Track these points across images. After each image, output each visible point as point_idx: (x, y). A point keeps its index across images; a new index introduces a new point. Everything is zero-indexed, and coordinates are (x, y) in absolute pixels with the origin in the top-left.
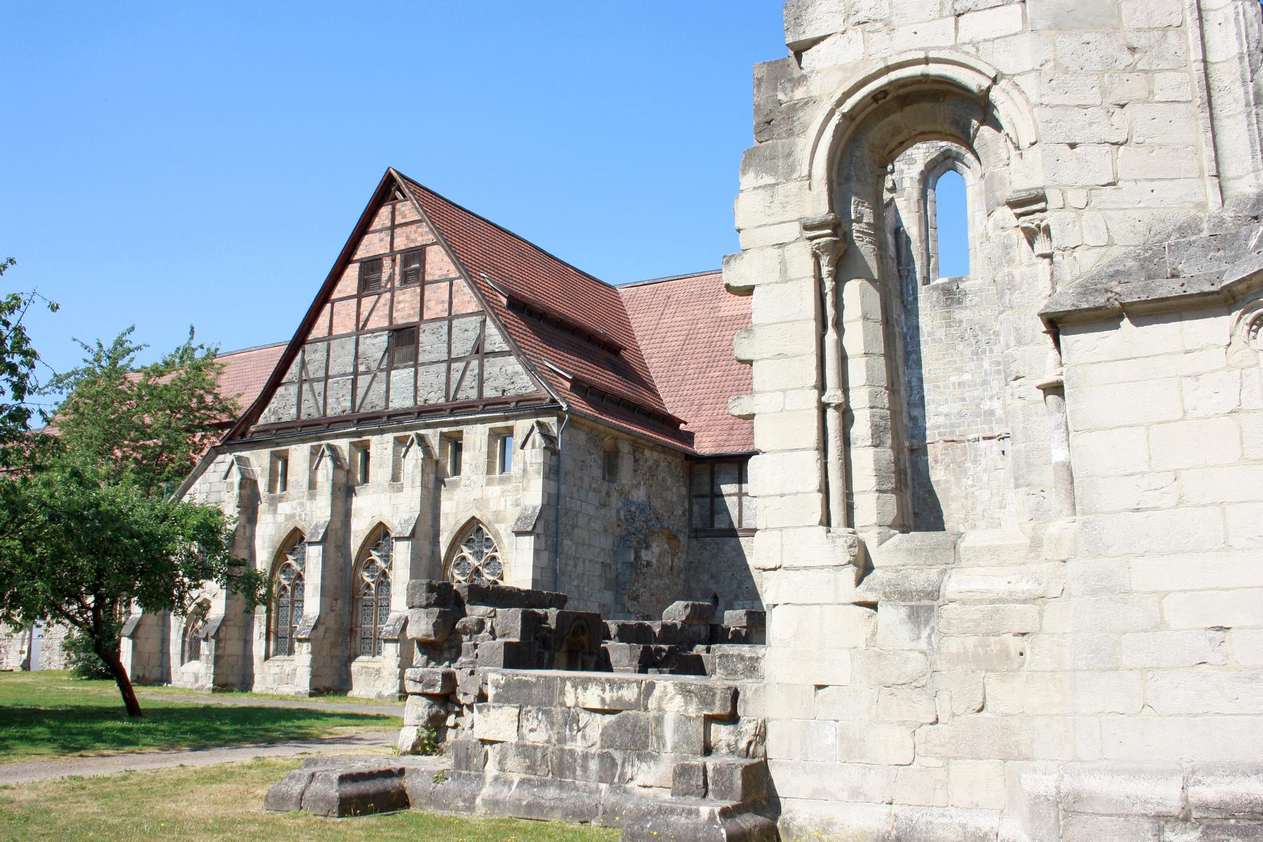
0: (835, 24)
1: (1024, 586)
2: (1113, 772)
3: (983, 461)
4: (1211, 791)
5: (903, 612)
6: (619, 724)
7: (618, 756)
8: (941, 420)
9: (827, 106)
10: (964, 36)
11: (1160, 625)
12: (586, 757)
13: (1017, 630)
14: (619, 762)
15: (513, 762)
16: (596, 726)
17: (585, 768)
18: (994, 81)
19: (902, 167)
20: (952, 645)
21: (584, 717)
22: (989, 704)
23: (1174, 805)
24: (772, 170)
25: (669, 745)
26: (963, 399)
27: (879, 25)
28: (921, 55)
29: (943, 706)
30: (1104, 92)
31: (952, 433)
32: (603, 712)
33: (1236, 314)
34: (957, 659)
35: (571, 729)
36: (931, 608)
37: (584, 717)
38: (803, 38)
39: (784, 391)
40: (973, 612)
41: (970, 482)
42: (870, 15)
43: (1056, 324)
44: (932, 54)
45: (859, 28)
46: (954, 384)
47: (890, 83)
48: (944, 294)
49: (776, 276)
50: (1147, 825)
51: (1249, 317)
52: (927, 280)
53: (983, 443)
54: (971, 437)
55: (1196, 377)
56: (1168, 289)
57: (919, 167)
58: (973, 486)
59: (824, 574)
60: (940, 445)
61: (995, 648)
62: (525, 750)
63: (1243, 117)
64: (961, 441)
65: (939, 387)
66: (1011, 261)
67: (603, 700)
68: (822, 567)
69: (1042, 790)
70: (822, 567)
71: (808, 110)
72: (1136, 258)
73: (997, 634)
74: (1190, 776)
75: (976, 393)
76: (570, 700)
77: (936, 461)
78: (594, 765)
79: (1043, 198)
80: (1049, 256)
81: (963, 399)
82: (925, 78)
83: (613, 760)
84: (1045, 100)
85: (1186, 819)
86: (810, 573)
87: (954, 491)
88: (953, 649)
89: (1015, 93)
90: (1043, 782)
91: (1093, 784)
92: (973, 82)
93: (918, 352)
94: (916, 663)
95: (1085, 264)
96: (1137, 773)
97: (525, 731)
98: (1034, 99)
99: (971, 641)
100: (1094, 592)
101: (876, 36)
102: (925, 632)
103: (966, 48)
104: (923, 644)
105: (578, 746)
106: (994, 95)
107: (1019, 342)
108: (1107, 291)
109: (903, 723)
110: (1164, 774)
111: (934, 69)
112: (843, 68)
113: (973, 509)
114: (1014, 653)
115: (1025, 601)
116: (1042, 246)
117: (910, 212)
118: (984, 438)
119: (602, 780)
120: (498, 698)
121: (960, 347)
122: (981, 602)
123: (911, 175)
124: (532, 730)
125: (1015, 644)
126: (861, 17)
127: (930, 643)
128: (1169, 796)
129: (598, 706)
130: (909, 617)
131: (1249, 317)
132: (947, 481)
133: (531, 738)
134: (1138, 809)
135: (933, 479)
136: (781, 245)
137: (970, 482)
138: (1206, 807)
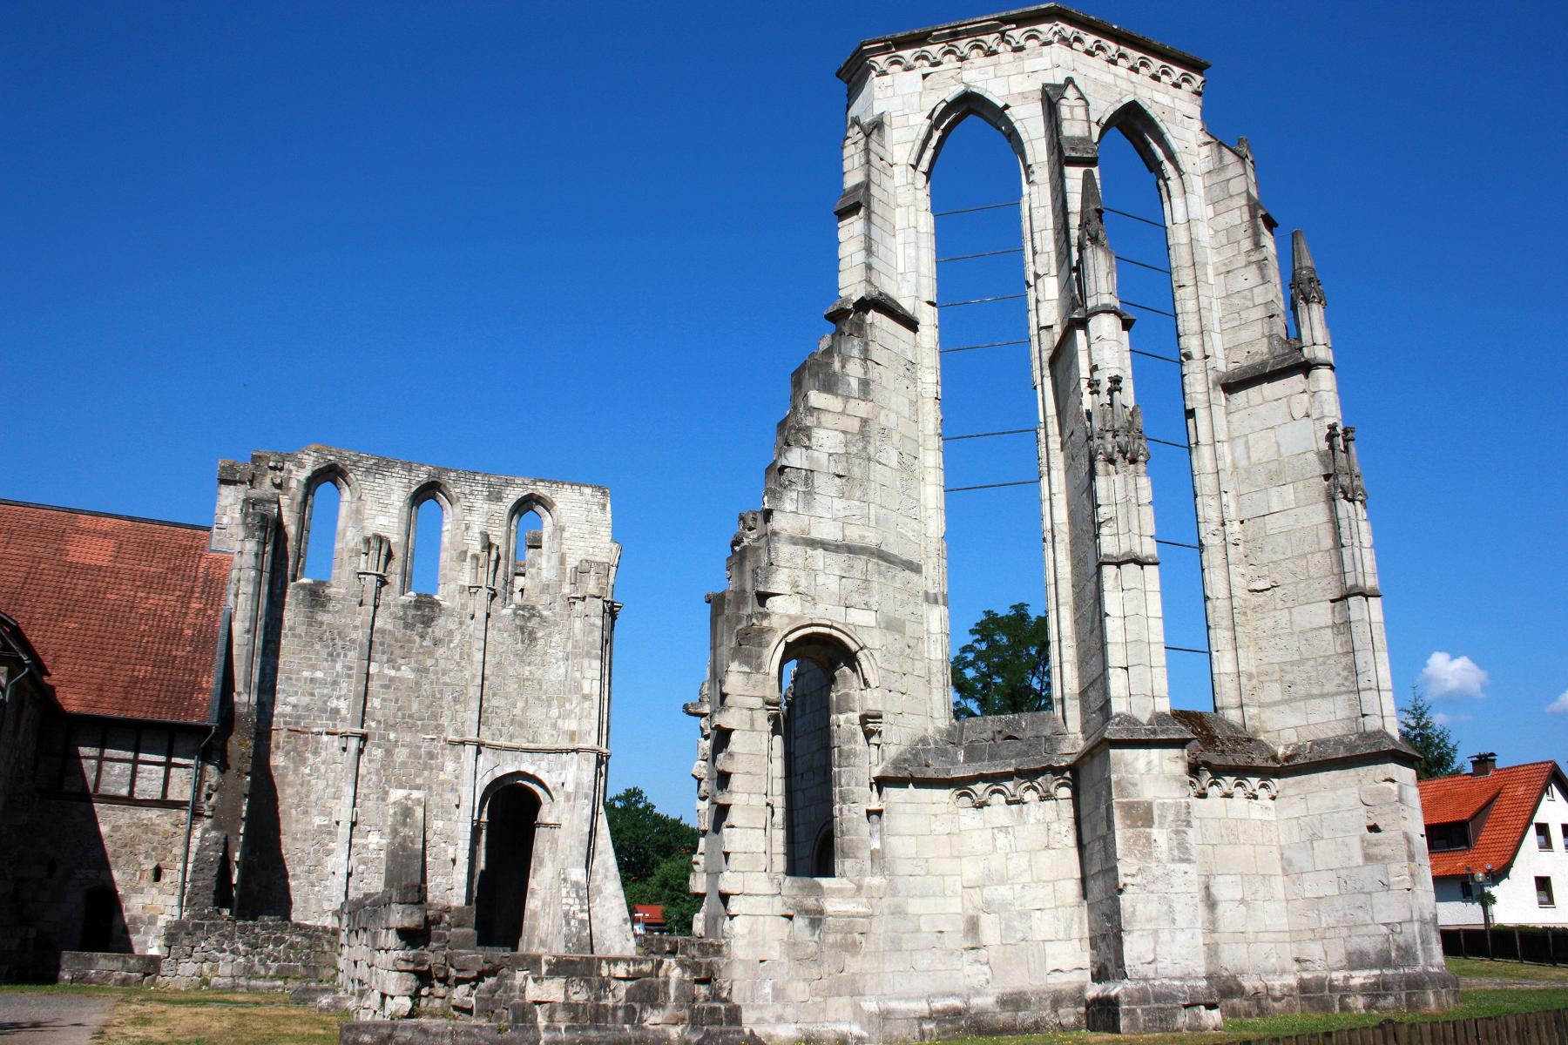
0: (785, 589)
1: (862, 910)
2: (899, 999)
3: (323, 754)
4: (939, 1004)
5: (807, 921)
6: (640, 986)
7: (637, 1006)
8: (288, 709)
9: (780, 635)
10: (850, 620)
11: (918, 930)
12: (615, 1008)
13: (860, 931)
14: (638, 1010)
15: (559, 1015)
16: (622, 989)
17: (614, 1016)
18: (861, 649)
19: (292, 468)
20: (830, 939)
21: (614, 984)
22: (846, 970)
23: (926, 1012)
24: (748, 664)
25: (672, 998)
26: (312, 695)
27: (809, 598)
28: (830, 623)
29: (825, 969)
30: (901, 667)
31: (297, 723)
32: (625, 979)
33: (952, 790)
34: (832, 946)
35: (605, 991)
36: (821, 919)
37: (614, 984)
38: (769, 591)
39: (749, 794)
40: (841, 922)
41: (307, 771)
42: (805, 590)
43: (881, 783)
44: (835, 625)
45: (799, 596)
46: (306, 679)
47: (813, 634)
48: (311, 595)
49: (747, 727)
50: (916, 1022)
51: (958, 792)
52: (294, 579)
53: (325, 738)
54: (315, 730)
55: (936, 816)
56: (930, 773)
57: (304, 474)
58: (310, 775)
59: (766, 899)
60: (284, 733)
61: (850, 941)
62: (569, 1007)
63: (941, 690)
64: (304, 733)
65: (291, 679)
66: (856, 742)
67: (628, 972)
68: (765, 895)
69: (873, 1010)
70: (765, 895)
71: (771, 633)
72: (910, 752)
73: (851, 933)
74: (929, 998)
75: (326, 691)
76: (605, 972)
77: (278, 747)
78: (620, 1013)
79: (881, 717)
80: (878, 746)
81: (312, 695)
82: (830, 636)
83: (634, 1009)
84: (883, 665)
85: (930, 1018)
86: (759, 898)
87: (291, 777)
88: (831, 941)
89: (870, 658)
90: (871, 1006)
91: (893, 1005)
92: (854, 647)
93: (278, 643)
94: (812, 948)
95: (892, 752)
96: (907, 999)
97: (570, 993)
98: (879, 664)
99: (839, 937)
100: (893, 914)
101: (808, 605)
102: (817, 933)
103: (851, 627)
104: (816, 938)
105: (610, 1002)
106: (860, 655)
107: (857, 785)
108: (906, 769)
109: (805, 980)
110: (919, 999)
111: (835, 633)
112: (789, 616)
113: (307, 796)
114: (858, 942)
115: (864, 917)
116: (875, 740)
117: (291, 511)
118: (327, 733)
119: (626, 1023)
120: (549, 972)
121: (317, 647)
122: (844, 917)
123: (299, 478)
124: (575, 993)
125: (858, 937)
126: (800, 589)
127: (819, 937)
128: (922, 1007)
129: (625, 976)
130: (810, 923)
131: (958, 792)
132: (285, 767)
133: (575, 998)
134: (913, 1015)
135: (272, 763)
136: (751, 709)
137: (307, 771)
138: (938, 1012)
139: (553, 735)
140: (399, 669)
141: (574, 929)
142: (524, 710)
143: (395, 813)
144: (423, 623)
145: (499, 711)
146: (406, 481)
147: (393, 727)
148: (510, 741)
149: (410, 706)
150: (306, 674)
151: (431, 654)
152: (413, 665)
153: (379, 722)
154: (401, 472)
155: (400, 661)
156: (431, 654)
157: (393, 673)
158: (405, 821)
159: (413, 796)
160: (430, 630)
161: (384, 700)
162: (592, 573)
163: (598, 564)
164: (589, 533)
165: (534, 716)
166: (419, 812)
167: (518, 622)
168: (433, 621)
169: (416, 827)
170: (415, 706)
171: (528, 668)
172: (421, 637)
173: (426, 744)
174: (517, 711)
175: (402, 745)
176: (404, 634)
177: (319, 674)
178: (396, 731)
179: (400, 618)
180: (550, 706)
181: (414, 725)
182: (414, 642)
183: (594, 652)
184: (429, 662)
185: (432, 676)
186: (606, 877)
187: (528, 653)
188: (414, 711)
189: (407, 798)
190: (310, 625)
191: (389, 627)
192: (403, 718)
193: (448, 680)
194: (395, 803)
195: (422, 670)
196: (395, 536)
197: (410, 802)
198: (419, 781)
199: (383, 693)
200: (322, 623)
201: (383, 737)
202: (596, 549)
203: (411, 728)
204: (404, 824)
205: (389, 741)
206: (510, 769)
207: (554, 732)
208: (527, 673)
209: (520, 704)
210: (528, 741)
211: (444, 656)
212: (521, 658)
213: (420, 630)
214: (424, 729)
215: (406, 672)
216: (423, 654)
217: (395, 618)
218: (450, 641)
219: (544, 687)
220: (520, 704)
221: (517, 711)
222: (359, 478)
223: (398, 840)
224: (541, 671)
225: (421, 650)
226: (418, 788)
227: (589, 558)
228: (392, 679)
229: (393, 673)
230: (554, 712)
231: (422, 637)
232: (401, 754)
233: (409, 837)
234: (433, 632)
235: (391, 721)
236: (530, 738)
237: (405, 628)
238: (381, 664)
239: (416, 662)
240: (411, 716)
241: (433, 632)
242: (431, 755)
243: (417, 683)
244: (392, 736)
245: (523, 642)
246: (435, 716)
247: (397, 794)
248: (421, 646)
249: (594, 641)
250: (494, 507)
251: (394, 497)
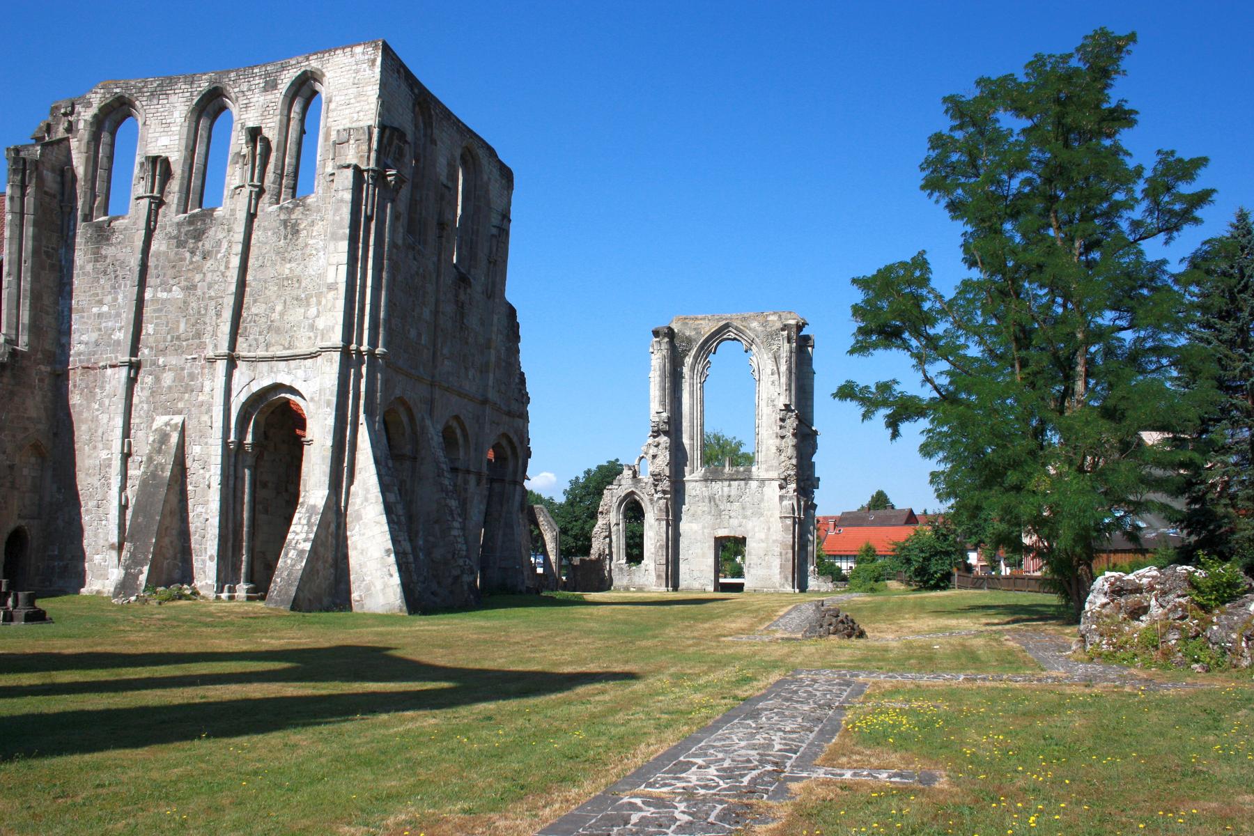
3: (107, 387)
8: (82, 347)
19: (80, 110)
26: (100, 330)
31: (89, 360)
41: (97, 406)
48: (96, 231)
52: (88, 217)
53: (109, 371)
54: (101, 364)
57: (94, 110)
58: (98, 410)
60: (79, 371)
65: (83, 317)
75: (110, 324)
77: (75, 386)
81: (100, 330)
87: (85, 415)
93: (71, 284)
113: (96, 431)
117: (80, 152)
121: (102, 281)
123: (86, 118)
132: (81, 405)
135: (71, 402)
137: (97, 406)
139: (310, 338)
140: (171, 291)
141: (289, 561)
142: (282, 314)
143: (154, 441)
144: (194, 238)
145: (257, 319)
146: (188, 94)
147: (163, 352)
148: (267, 351)
149: (178, 327)
150: (95, 310)
151: (198, 269)
152: (183, 284)
153: (151, 348)
154: (183, 87)
155: (171, 282)
156: (198, 269)
157: (165, 295)
158: (160, 448)
159: (172, 422)
160: (200, 244)
161: (157, 325)
162: (352, 142)
163: (357, 129)
164: (355, 98)
165: (291, 318)
166: (174, 438)
167: (283, 217)
168: (204, 234)
169: (169, 453)
170: (182, 327)
171: (288, 266)
172: (191, 253)
173: (189, 365)
174: (275, 316)
175: (169, 370)
176: (176, 254)
177: (105, 308)
178: (165, 355)
179: (174, 237)
180: (308, 305)
181: (180, 347)
182: (183, 260)
183: (341, 231)
184: (198, 277)
185: (199, 292)
186: (366, 500)
187: (290, 248)
188: (181, 331)
189: (167, 424)
190: (96, 261)
191: (163, 248)
192: (172, 341)
193: (213, 294)
194: (156, 430)
195: (190, 288)
196: (176, 154)
197: (168, 428)
198: (180, 405)
199: (157, 318)
200: (106, 257)
201: (154, 363)
202: (361, 114)
203: (178, 351)
204: (159, 451)
205: (159, 366)
206: (266, 382)
207: (312, 334)
208: (287, 271)
209: (279, 308)
210: (285, 348)
211: (211, 268)
212: (282, 256)
213: (192, 246)
214: (188, 350)
215: (177, 293)
216: (192, 270)
217: (170, 238)
218: (218, 252)
219: (303, 285)
220: (279, 308)
221: (275, 316)
222: (144, 103)
223: (152, 468)
224: (301, 266)
225: (191, 267)
226: (180, 412)
227: (354, 125)
228: (164, 301)
229: (165, 295)
230: (313, 311)
231: (193, 253)
232: (168, 379)
233: (161, 464)
234: (203, 246)
235: (162, 346)
236: (287, 345)
237: (178, 247)
238: (155, 288)
239: (186, 280)
240: (178, 338)
241: (203, 246)
242: (192, 377)
243: (185, 302)
244: (161, 361)
245: (285, 238)
246: (198, 335)
247: (160, 421)
248: (191, 263)
249: (342, 219)
250: (269, 97)
251: (176, 114)
